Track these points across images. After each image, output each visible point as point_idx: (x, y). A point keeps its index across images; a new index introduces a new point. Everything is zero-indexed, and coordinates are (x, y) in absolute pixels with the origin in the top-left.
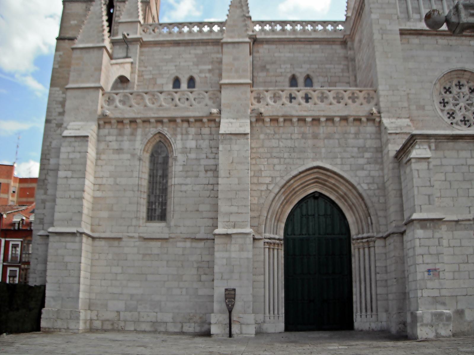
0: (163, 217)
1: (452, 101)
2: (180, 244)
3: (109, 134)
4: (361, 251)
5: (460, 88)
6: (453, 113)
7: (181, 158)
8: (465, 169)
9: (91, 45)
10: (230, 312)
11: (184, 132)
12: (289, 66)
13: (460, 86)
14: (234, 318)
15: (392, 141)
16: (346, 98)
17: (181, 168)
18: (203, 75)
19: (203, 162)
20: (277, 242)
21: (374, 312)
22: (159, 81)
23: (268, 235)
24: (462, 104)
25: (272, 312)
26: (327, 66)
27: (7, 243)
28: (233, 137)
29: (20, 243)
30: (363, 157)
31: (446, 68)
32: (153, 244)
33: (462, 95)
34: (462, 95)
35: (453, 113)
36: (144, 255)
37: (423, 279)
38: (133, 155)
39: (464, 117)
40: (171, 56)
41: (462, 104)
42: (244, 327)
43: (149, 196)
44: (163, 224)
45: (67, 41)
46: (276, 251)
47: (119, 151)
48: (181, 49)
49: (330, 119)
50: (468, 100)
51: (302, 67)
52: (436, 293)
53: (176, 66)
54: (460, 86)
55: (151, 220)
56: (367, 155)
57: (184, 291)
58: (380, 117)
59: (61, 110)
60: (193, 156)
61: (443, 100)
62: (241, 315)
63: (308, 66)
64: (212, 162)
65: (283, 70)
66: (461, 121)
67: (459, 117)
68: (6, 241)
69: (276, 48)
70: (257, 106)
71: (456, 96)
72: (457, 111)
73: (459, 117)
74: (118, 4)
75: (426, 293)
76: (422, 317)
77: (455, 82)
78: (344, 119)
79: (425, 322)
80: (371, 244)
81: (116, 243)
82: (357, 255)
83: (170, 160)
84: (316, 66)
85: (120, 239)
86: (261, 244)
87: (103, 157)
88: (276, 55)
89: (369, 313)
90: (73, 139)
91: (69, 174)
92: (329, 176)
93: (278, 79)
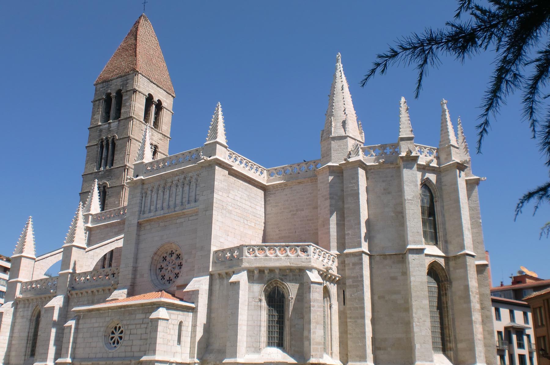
24: (169, 268)
74: (108, 190)
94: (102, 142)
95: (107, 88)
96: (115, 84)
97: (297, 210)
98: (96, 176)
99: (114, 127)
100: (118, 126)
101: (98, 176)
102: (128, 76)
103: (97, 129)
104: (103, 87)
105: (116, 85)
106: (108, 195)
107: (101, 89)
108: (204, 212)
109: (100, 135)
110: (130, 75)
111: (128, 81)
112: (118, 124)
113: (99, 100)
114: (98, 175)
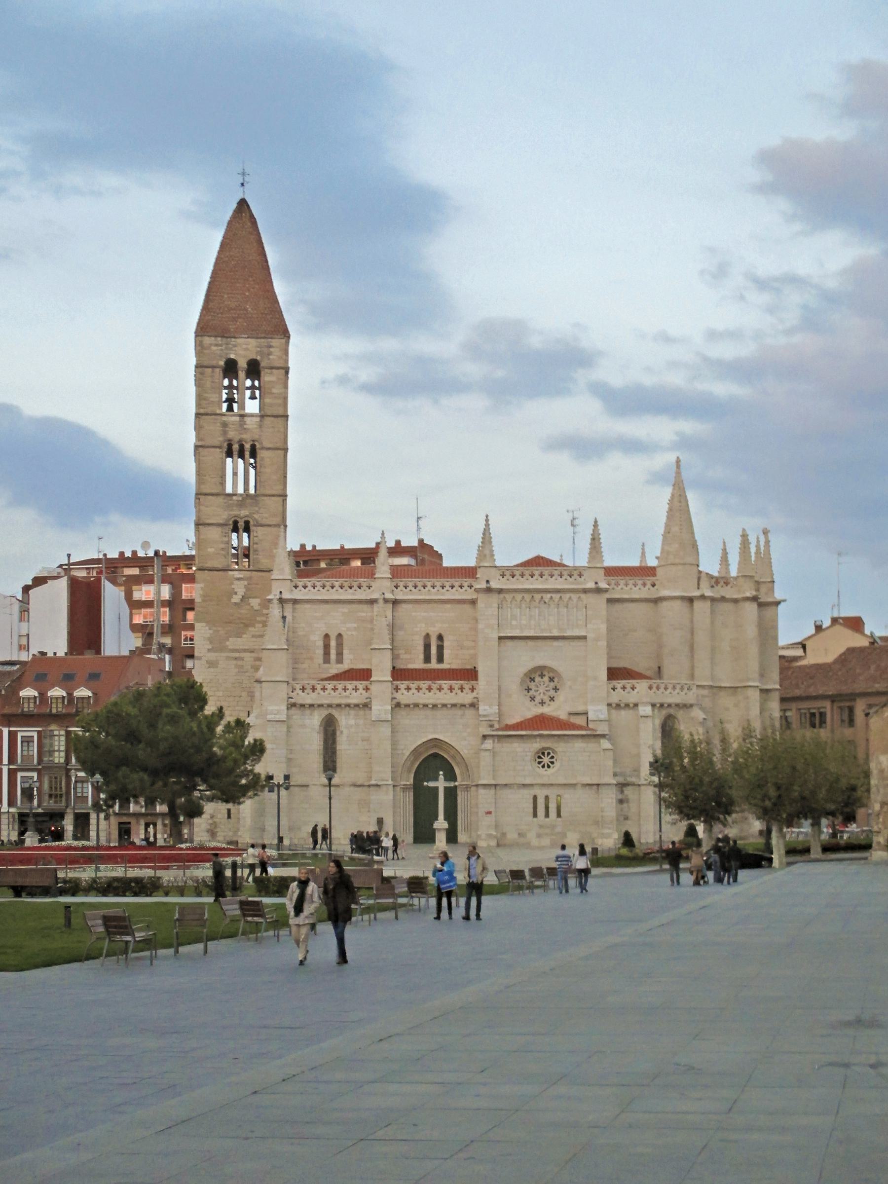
7: (345, 732)
12: (424, 625)
18: (350, 633)
23: (402, 783)
27: (12, 736)
28: (381, 723)
29: (35, 735)
31: (531, 665)
33: (542, 684)
34: (542, 684)
39: (542, 700)
45: (206, 571)
49: (444, 705)
50: (546, 687)
51: (435, 627)
53: (325, 623)
54: (542, 676)
56: (469, 730)
58: (478, 704)
59: (210, 647)
60: (353, 730)
65: (419, 629)
66: (540, 703)
67: (538, 699)
68: (10, 732)
71: (538, 685)
73: (538, 699)
78: (454, 705)
80: (468, 789)
81: (305, 788)
83: (338, 733)
84: (447, 625)
85: (307, 786)
86: (398, 789)
91: (274, 746)
94: (230, 446)
95: (226, 348)
96: (244, 346)
98: (226, 501)
99: (252, 424)
100: (261, 426)
101: (230, 502)
102: (270, 340)
103: (217, 419)
104: (217, 345)
105: (246, 349)
106: (257, 537)
107: (214, 348)
109: (225, 433)
111: (272, 350)
112: (261, 421)
113: (213, 367)
114: (231, 500)
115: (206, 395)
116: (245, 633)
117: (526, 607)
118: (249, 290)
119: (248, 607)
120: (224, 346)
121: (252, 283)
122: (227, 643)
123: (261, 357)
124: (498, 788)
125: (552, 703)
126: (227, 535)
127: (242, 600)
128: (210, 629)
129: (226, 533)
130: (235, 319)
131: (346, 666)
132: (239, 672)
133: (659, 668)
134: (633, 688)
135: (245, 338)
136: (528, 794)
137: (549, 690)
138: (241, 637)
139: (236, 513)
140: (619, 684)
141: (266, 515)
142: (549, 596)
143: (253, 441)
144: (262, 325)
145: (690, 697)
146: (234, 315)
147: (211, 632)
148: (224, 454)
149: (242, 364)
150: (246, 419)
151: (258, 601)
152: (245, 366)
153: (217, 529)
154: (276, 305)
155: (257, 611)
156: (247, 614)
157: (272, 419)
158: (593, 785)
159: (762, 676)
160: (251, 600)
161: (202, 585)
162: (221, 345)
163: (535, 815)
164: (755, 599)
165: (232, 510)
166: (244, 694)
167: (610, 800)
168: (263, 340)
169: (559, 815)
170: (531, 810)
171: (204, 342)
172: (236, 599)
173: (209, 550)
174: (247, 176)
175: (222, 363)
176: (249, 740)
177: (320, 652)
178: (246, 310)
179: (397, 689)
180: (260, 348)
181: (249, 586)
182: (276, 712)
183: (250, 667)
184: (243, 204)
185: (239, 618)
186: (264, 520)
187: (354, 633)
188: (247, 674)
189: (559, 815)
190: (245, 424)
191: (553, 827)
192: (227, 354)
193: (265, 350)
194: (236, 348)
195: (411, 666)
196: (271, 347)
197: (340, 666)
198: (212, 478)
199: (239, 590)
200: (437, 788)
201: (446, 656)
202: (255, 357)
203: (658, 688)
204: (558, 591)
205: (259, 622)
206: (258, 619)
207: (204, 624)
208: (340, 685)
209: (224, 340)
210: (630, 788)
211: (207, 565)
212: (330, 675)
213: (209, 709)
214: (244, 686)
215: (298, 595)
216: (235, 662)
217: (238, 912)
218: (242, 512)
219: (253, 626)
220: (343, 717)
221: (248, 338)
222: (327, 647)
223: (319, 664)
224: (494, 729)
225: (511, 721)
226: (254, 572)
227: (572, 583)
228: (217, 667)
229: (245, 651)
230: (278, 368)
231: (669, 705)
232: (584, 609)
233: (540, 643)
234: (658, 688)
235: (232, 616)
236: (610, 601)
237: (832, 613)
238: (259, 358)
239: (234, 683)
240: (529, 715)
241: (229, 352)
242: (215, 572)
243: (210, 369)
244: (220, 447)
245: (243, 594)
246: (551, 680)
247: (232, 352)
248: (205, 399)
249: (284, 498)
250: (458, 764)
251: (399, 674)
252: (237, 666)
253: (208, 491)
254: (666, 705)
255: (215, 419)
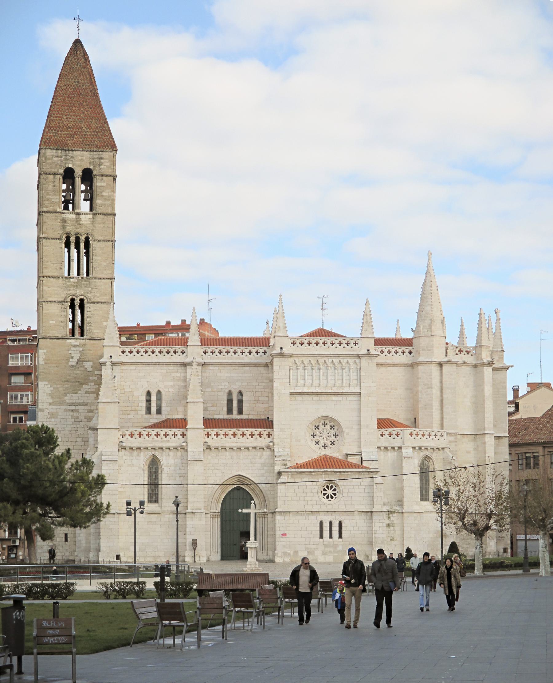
0: (156, 501)
1: (318, 434)
2: (167, 516)
3: (125, 455)
4: (261, 519)
5: (325, 426)
6: (318, 442)
8: (305, 487)
9: (109, 401)
10: (195, 550)
11: (167, 455)
12: (227, 384)
13: (325, 424)
14: (196, 553)
15: (277, 464)
16: (256, 435)
17: (166, 475)
18: (167, 390)
19: (178, 472)
20: (217, 514)
21: (266, 551)
22: (136, 394)
23: (212, 511)
24: (324, 436)
25: (214, 550)
26: (254, 384)
28: (195, 462)
30: (263, 469)
31: (316, 416)
32: (152, 516)
33: (325, 430)
34: (325, 430)
35: (318, 442)
36: (148, 522)
37: (279, 538)
38: (139, 468)
39: (325, 444)
40: (144, 374)
41: (324, 436)
42: (201, 557)
43: (149, 490)
44: (156, 505)
45: (48, 340)
46: (216, 519)
47: (131, 465)
48: (151, 368)
52: (284, 543)
54: (325, 424)
55: (150, 502)
56: (266, 468)
57: (170, 540)
59: (51, 401)
61: (314, 433)
62: (200, 552)
63: (240, 384)
64: (183, 472)
65: (223, 387)
66: (323, 446)
67: (322, 443)
69: (219, 369)
70: (207, 440)
71: (322, 431)
72: (321, 441)
73: (322, 443)
75: (280, 543)
76: (277, 553)
77: (322, 422)
79: (279, 555)
80: (266, 516)
82: (259, 521)
83: (160, 471)
86: (209, 515)
87: (122, 468)
88: (218, 374)
89: (264, 551)
90: (109, 462)
92: (245, 479)
93: (220, 394)
94: (68, 238)
95: (65, 159)
96: (80, 158)
97: (392, 389)
98: (64, 282)
99: (86, 221)
100: (93, 222)
101: (69, 283)
102: (101, 153)
104: (57, 156)
105: (82, 160)
106: (90, 312)
107: (55, 159)
108: (367, 397)
109: (64, 227)
110: (104, 153)
111: (102, 161)
112: (93, 218)
113: (55, 174)
114: (69, 282)
115: (48, 197)
116: (80, 390)
117: (312, 369)
118: (83, 113)
119: (82, 369)
120: (64, 157)
121: (86, 107)
122: (66, 398)
123: (94, 167)
124: (291, 514)
125: (332, 446)
126: (66, 310)
127: (77, 363)
128: (51, 387)
129: (64, 308)
130: (72, 136)
131: (163, 417)
132: (75, 422)
133: (415, 419)
134: (398, 435)
135: (81, 151)
136: (316, 520)
137: (331, 436)
138: (76, 393)
139: (72, 292)
140: (386, 431)
141: (98, 295)
142: (330, 360)
143: (87, 234)
144: (94, 141)
145: (442, 442)
146: (71, 133)
147: (52, 389)
148: (63, 245)
149: (78, 172)
150: (81, 216)
151: (91, 363)
152: (81, 173)
153: (58, 305)
154: (106, 125)
155: (90, 371)
156: (82, 374)
157: (103, 216)
158: (368, 512)
159: (495, 426)
160: (85, 363)
161: (45, 351)
162: (61, 157)
163: (321, 537)
164: (490, 364)
165: (69, 290)
166: (79, 440)
167: (381, 525)
168: (95, 153)
169: (340, 537)
170: (319, 532)
171: (47, 154)
172: (73, 362)
173: (51, 322)
174: (81, 21)
175: (62, 171)
176: (94, 474)
177: (144, 405)
178: (82, 128)
179: (208, 435)
180: (93, 159)
181: (84, 352)
182: (109, 454)
183: (84, 418)
184: (77, 43)
185: (75, 378)
186: (96, 298)
187: (170, 390)
188: (81, 423)
189: (340, 537)
190: (80, 221)
191: (335, 546)
192: (66, 164)
193: (97, 161)
194: (73, 159)
195: (216, 417)
196: (101, 158)
197: (159, 416)
198: (53, 264)
199: (75, 355)
200: (248, 515)
201: (245, 409)
202: (89, 167)
203: (417, 435)
204: (338, 356)
205: (92, 381)
206: (91, 378)
207: (46, 383)
208: (162, 432)
209: (63, 152)
210: (395, 514)
211: (49, 335)
212: (150, 424)
213: (58, 451)
214: (79, 433)
215: (125, 358)
216: (71, 413)
217: (155, 615)
218: (78, 292)
219: (86, 384)
220: (164, 457)
221: (83, 151)
222: (149, 401)
223: (142, 415)
224: (286, 467)
225: (301, 461)
226: (87, 340)
227: (350, 350)
228: (57, 418)
229: (80, 404)
230: (107, 176)
231: (426, 448)
232: (359, 371)
233: (323, 398)
234: (417, 435)
235: (70, 376)
236: (379, 365)
237: (527, 380)
238: (92, 167)
239: (71, 431)
240: (315, 456)
241: (69, 162)
242: (55, 340)
243: (52, 176)
244: (60, 239)
245: (78, 358)
246: (332, 427)
247: (70, 162)
248: (48, 200)
249: (112, 281)
250: (257, 495)
251: (208, 423)
252: (72, 416)
253: (50, 274)
254: (423, 448)
255: (56, 216)
